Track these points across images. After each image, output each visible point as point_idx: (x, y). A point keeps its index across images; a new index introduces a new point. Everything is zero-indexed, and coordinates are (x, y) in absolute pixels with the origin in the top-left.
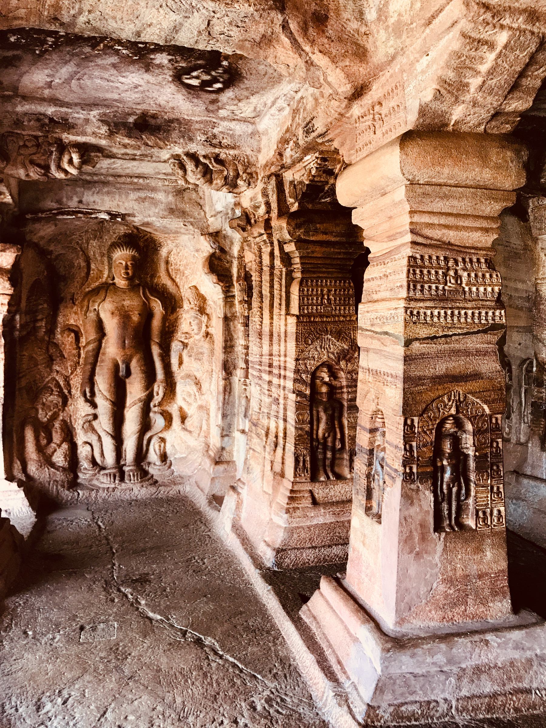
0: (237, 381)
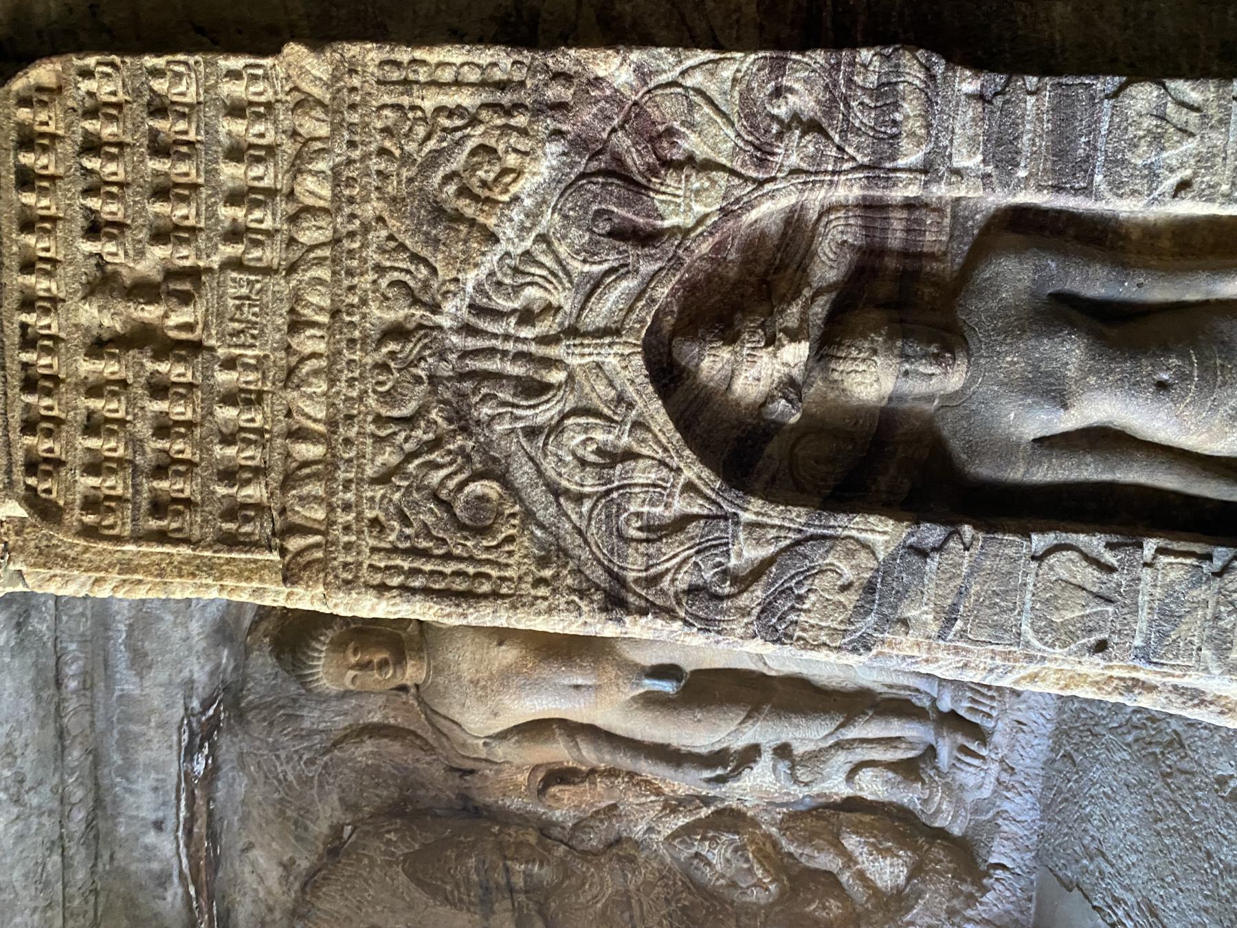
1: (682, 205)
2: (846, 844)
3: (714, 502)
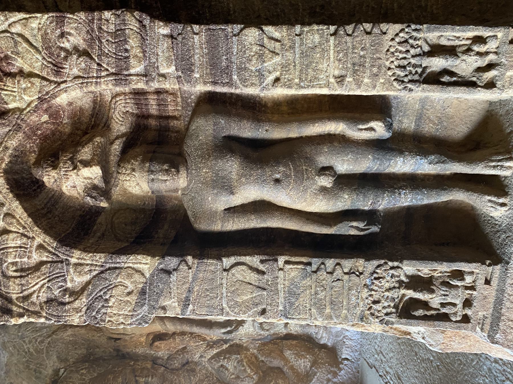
2: (285, 355)
3: (54, 254)
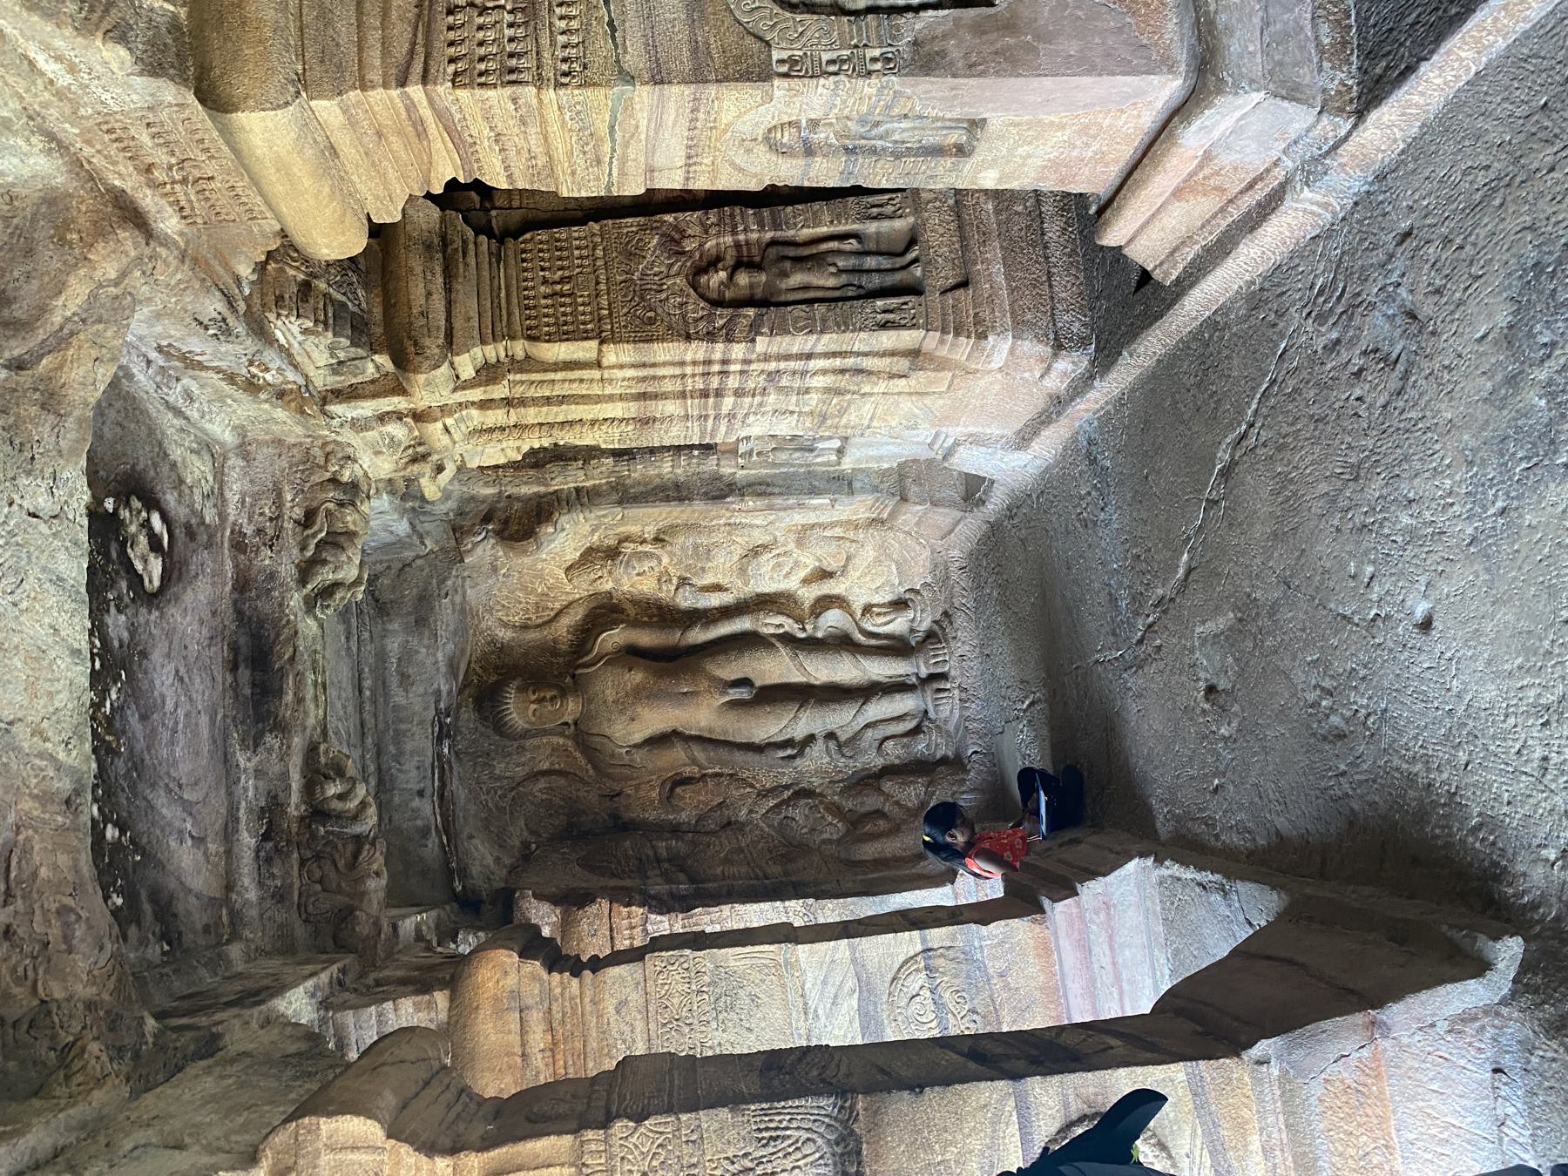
0: (741, 472)
1: (689, 245)
